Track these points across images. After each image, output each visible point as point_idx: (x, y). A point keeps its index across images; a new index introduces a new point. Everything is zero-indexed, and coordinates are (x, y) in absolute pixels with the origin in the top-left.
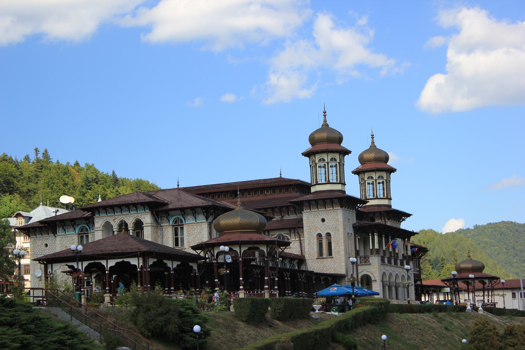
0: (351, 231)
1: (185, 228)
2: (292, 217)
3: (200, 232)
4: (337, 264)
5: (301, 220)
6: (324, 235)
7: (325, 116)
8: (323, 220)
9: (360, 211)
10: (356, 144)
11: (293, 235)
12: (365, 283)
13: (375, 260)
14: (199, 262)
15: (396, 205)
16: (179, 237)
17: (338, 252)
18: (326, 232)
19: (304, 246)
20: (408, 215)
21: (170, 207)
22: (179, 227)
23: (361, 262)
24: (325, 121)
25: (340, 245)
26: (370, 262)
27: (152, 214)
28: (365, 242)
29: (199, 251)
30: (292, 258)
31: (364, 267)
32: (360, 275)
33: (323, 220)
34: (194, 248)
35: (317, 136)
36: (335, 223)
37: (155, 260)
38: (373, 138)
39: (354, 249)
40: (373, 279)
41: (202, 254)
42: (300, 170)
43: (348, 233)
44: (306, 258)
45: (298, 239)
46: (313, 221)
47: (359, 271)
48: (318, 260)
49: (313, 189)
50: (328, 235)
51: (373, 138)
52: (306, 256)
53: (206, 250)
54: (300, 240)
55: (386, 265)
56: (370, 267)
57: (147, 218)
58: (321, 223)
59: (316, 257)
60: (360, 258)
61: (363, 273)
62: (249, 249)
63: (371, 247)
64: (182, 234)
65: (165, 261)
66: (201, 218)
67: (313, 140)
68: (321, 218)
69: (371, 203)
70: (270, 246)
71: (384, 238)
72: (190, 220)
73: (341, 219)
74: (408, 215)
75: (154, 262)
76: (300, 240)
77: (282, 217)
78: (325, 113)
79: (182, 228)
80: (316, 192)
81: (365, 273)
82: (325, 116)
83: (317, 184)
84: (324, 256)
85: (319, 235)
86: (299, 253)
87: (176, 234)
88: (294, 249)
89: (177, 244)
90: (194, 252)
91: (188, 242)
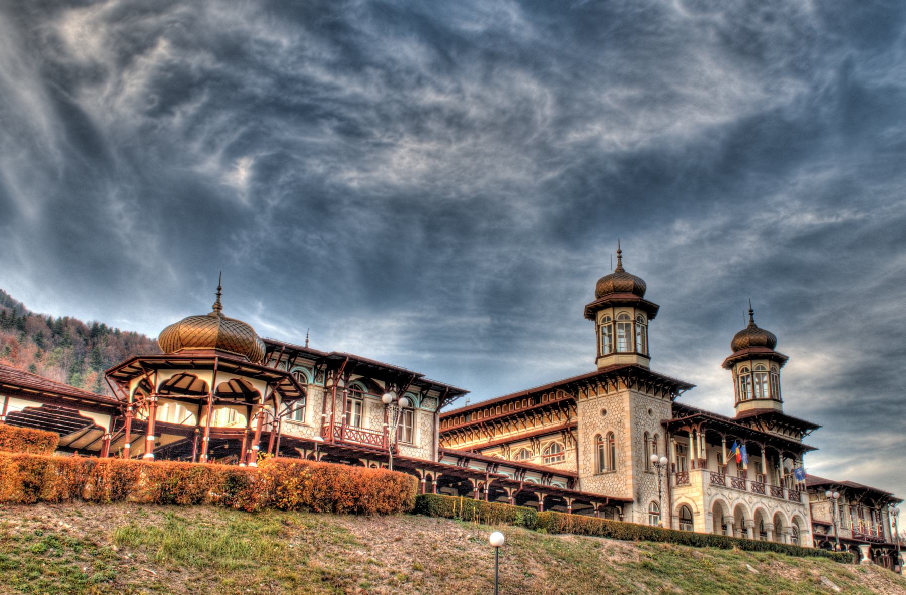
6: (604, 435)
7: (620, 257)
8: (604, 412)
11: (568, 443)
17: (624, 462)
18: (606, 431)
20: (814, 427)
23: (678, 483)
24: (620, 265)
26: (691, 480)
28: (682, 450)
32: (676, 505)
33: (604, 412)
40: (694, 510)
43: (646, 434)
45: (574, 447)
47: (675, 497)
48: (596, 478)
50: (611, 434)
51: (752, 315)
52: (581, 471)
55: (727, 489)
59: (593, 473)
60: (677, 476)
61: (680, 502)
67: (599, 295)
68: (600, 408)
71: (763, 455)
73: (627, 409)
74: (814, 427)
77: (569, 418)
81: (683, 500)
82: (620, 257)
85: (599, 436)
86: (574, 470)
88: (567, 465)
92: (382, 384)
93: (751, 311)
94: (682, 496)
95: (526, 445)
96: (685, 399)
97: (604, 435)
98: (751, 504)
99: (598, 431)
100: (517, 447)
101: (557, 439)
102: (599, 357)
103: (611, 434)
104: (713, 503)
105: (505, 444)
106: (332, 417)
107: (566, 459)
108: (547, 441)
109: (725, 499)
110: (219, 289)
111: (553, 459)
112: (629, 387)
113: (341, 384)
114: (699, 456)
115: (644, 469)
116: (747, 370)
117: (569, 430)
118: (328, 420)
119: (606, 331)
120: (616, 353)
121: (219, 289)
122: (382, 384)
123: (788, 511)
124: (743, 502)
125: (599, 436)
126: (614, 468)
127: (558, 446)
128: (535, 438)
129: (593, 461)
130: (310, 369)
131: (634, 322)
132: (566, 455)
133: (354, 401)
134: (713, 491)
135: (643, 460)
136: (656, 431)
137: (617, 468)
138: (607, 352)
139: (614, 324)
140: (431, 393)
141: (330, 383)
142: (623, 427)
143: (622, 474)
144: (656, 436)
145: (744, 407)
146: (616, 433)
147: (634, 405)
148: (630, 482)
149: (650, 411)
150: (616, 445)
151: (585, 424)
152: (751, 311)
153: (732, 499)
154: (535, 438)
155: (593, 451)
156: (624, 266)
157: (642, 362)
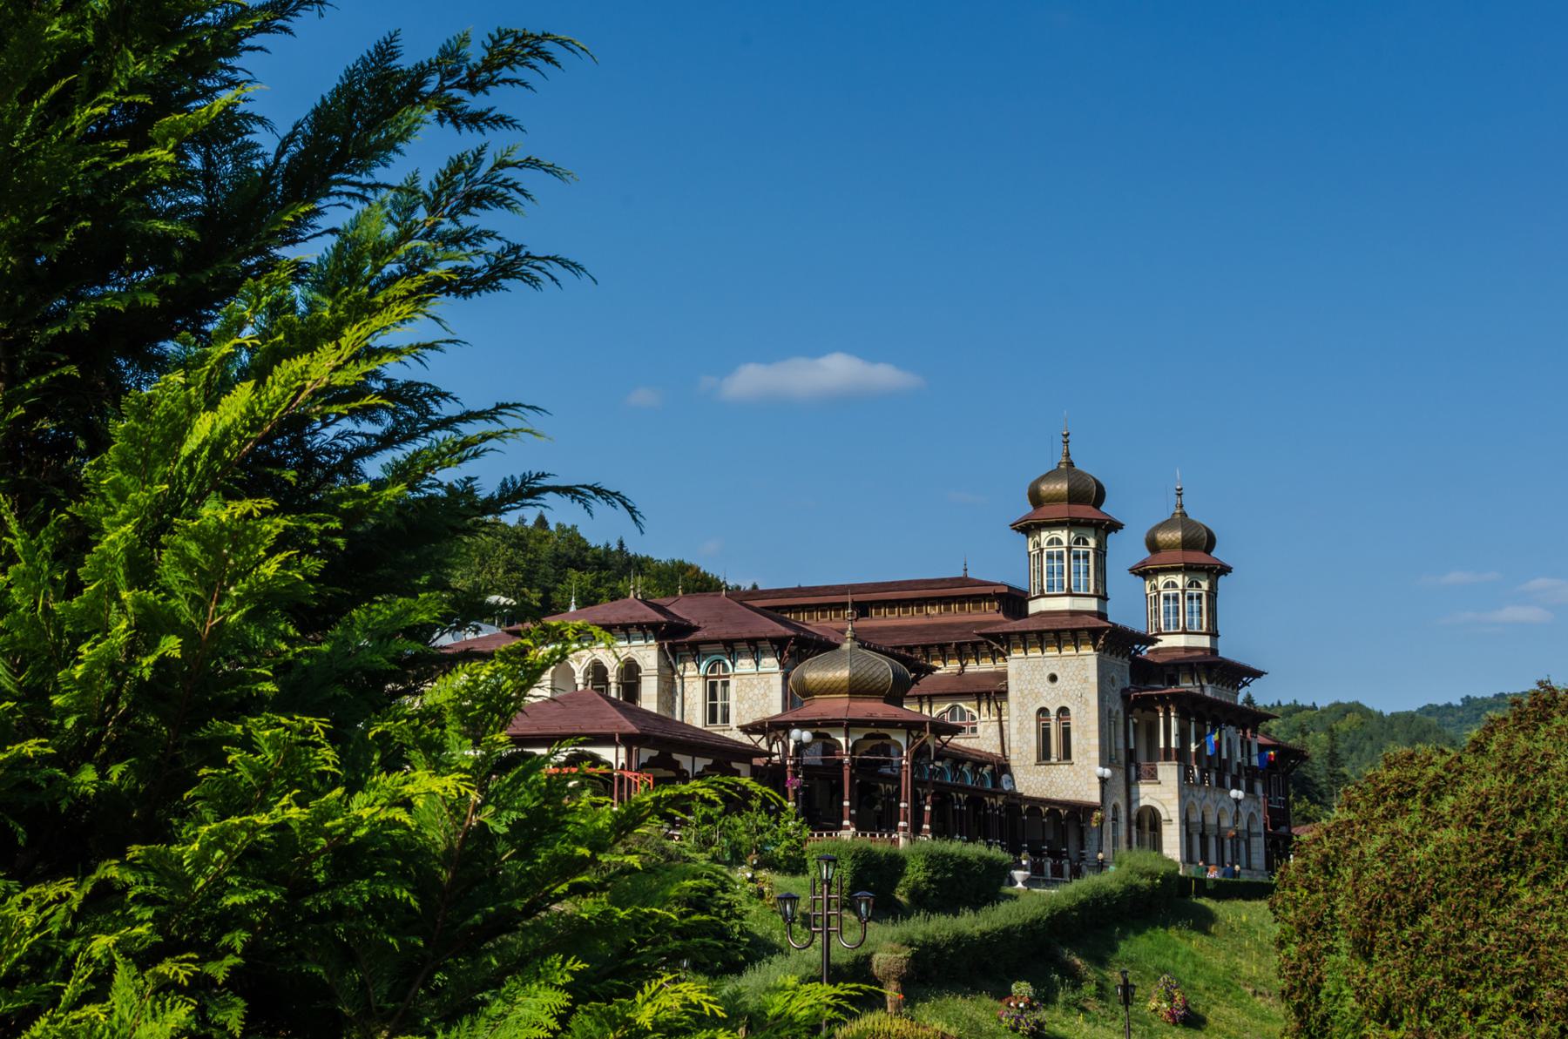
0: (1117, 707)
1: (733, 682)
2: (986, 666)
3: (765, 695)
4: (1079, 779)
5: (1003, 676)
6: (1053, 712)
8: (1053, 678)
9: (1144, 661)
10: (1138, 511)
12: (1147, 824)
14: (757, 761)
15: (1226, 652)
16: (719, 702)
17: (1085, 752)
20: (1257, 674)
21: (698, 635)
22: (719, 681)
26: (1160, 777)
27: (661, 649)
29: (756, 737)
30: (979, 761)
32: (1134, 808)
33: (1053, 678)
34: (745, 729)
36: (1070, 681)
37: (655, 753)
39: (1121, 745)
41: (763, 745)
42: (1000, 561)
49: (1034, 607)
50: (1063, 711)
53: (772, 735)
54: (1000, 721)
57: (647, 655)
58: (1049, 684)
59: (1034, 760)
62: (867, 737)
63: (1162, 745)
64: (725, 697)
65: (676, 756)
66: (770, 663)
69: (1167, 642)
70: (915, 733)
72: (745, 665)
74: (1257, 674)
75: (651, 758)
76: (1000, 721)
77: (963, 666)
79: (726, 684)
80: (1041, 614)
83: (1042, 595)
84: (1054, 760)
86: (997, 751)
87: (713, 696)
89: (713, 720)
90: (745, 739)
91: (739, 714)
97: (1053, 712)
99: (1043, 704)
129: (1034, 744)
132: (980, 727)
137: (1074, 758)
143: (1083, 768)
146: (1073, 711)
151: (1021, 691)
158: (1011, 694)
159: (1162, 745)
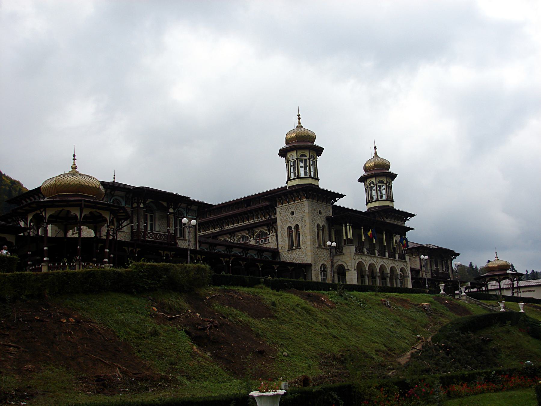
0: (322, 223)
4: (305, 254)
6: (293, 227)
7: (299, 118)
8: (293, 213)
13: (350, 251)
15: (398, 206)
19: (278, 241)
20: (412, 216)
23: (336, 253)
24: (299, 123)
25: (306, 235)
26: (344, 252)
31: (339, 257)
33: (293, 213)
35: (289, 136)
38: (375, 149)
40: (346, 268)
43: (318, 226)
44: (280, 251)
46: (284, 216)
50: (297, 226)
51: (375, 149)
52: (280, 248)
55: (365, 255)
56: (344, 257)
61: (338, 263)
63: (344, 238)
67: (287, 141)
73: (307, 211)
74: (412, 216)
77: (270, 216)
78: (299, 115)
81: (340, 263)
82: (299, 118)
85: (290, 228)
88: (272, 244)
92: (165, 204)
93: (375, 147)
94: (339, 260)
95: (245, 234)
96: (339, 203)
97: (293, 227)
98: (378, 262)
99: (289, 225)
100: (239, 235)
101: (264, 230)
102: (289, 180)
103: (297, 226)
104: (356, 263)
105: (232, 233)
106: (138, 226)
107: (270, 241)
108: (258, 231)
109: (363, 261)
110: (74, 156)
111: (262, 241)
112: (307, 198)
113: (142, 206)
114: (349, 237)
115: (317, 246)
116: (373, 183)
117: (272, 224)
118: (135, 227)
119: (292, 164)
120: (299, 177)
121: (74, 156)
122: (165, 204)
123: (398, 266)
124: (373, 262)
125: (290, 228)
126: (300, 246)
127: (265, 233)
128: (250, 229)
129: (287, 242)
130: (122, 197)
131: (309, 159)
132: (270, 239)
133: (149, 215)
134: (357, 257)
135: (317, 241)
136: (323, 223)
137: (301, 246)
138: (293, 177)
139: (297, 160)
140: (193, 207)
141: (135, 205)
142: (305, 222)
144: (323, 226)
145: (371, 205)
147: (311, 209)
148: (309, 254)
149: (320, 212)
150: (300, 233)
152: (375, 147)
153: (367, 261)
154: (250, 229)
155: (287, 236)
156: (302, 124)
157: (314, 182)
158: (278, 222)
159: (344, 238)
